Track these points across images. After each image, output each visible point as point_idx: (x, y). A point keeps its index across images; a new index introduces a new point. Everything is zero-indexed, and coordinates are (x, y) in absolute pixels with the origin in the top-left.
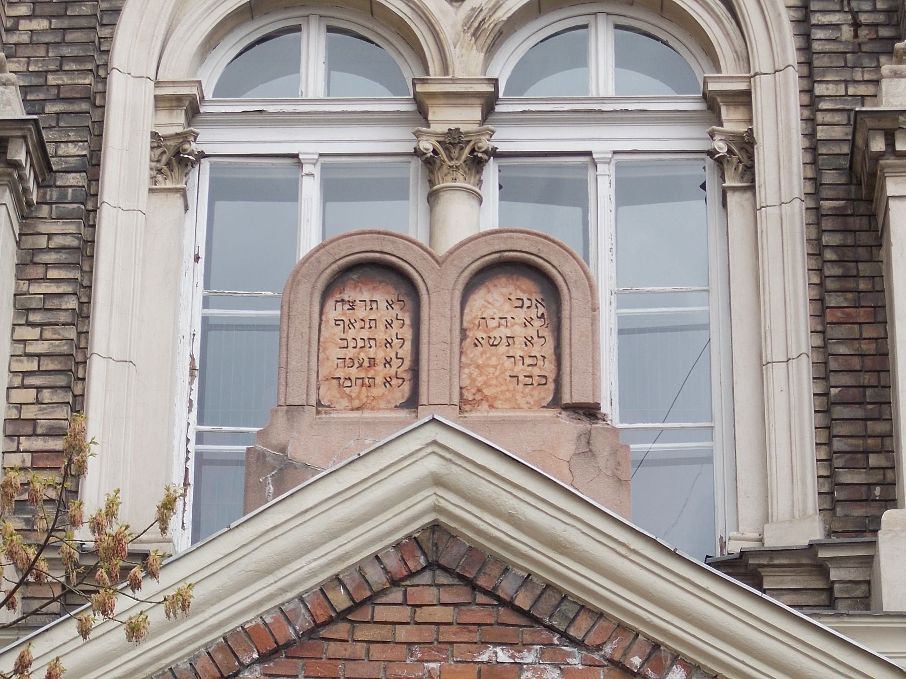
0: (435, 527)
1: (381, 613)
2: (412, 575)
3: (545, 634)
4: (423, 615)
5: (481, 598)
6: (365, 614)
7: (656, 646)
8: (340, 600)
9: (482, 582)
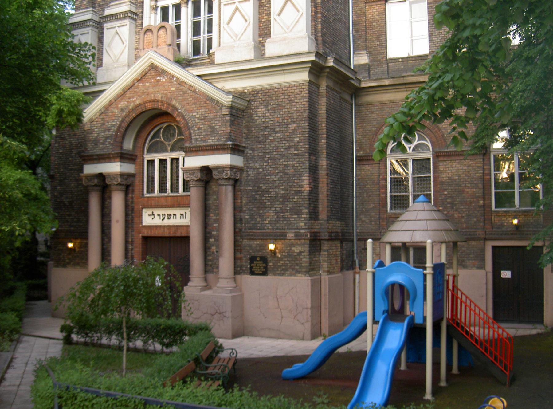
8: (144, 74)
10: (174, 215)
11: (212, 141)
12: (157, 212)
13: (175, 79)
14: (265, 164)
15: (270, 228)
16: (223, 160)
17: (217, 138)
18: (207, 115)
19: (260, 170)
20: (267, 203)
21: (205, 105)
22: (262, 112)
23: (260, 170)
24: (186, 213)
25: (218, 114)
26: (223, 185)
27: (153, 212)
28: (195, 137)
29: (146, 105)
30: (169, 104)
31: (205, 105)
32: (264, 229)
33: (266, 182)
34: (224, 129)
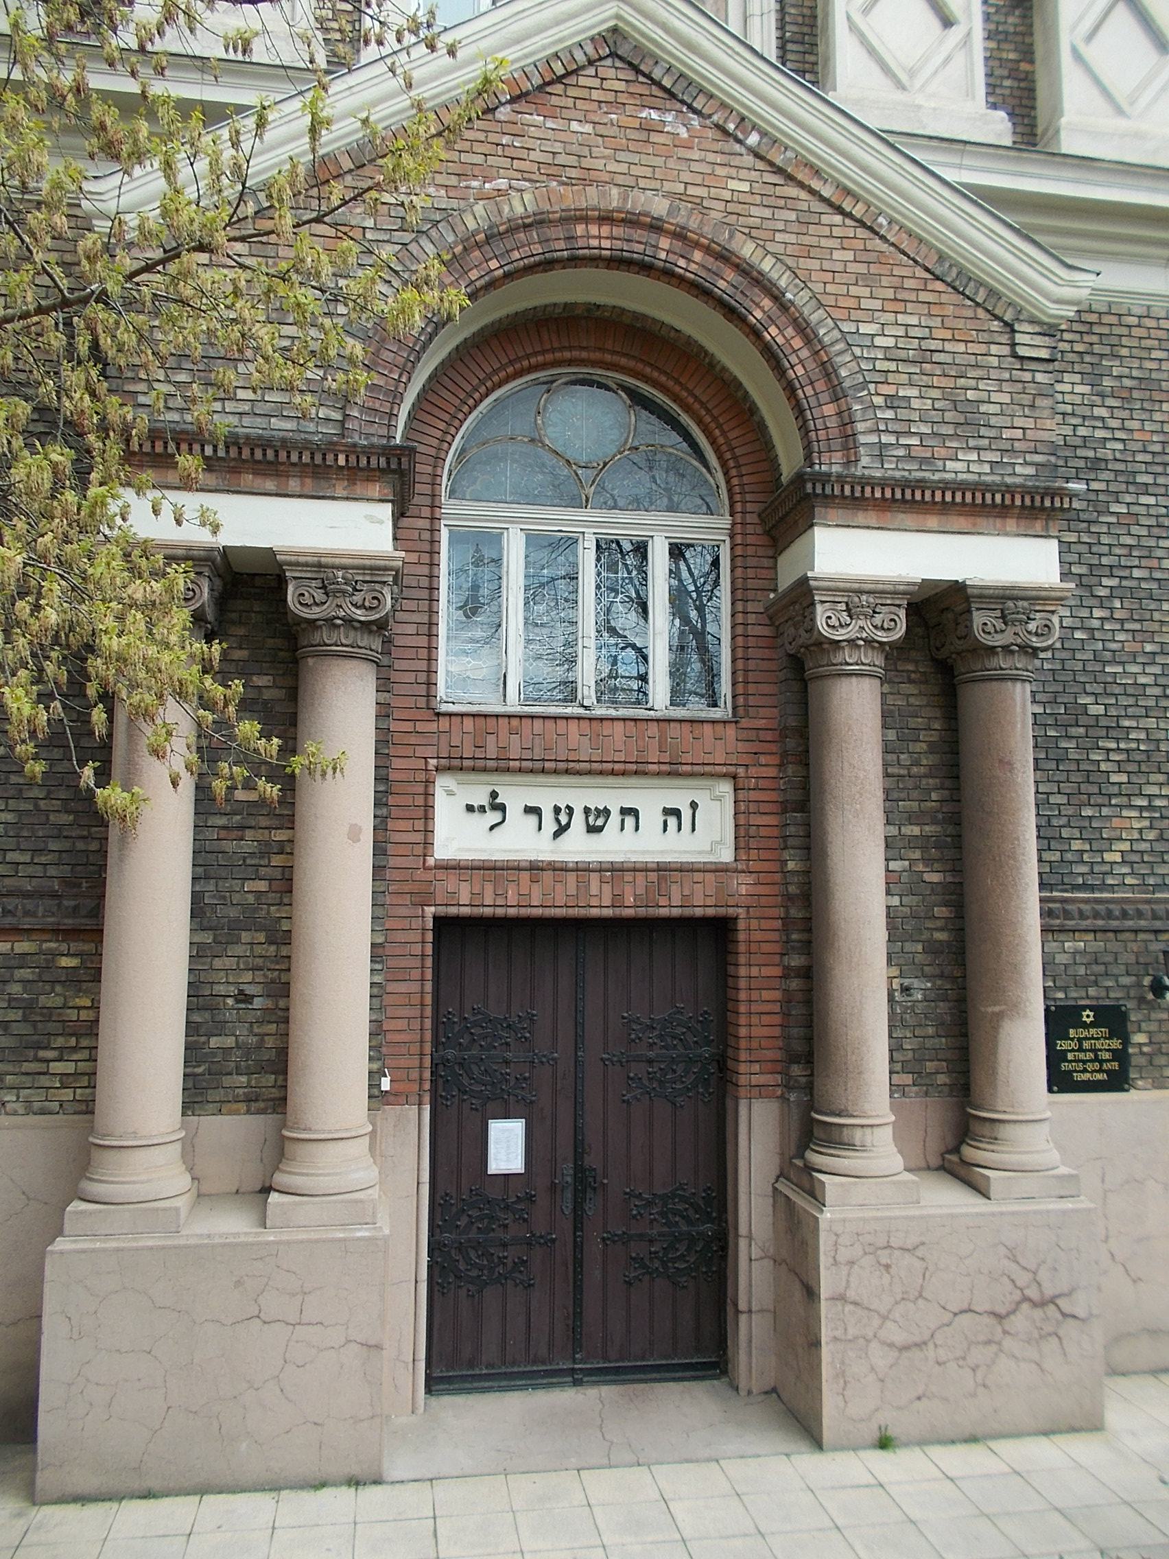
0: (615, 30)
1: (582, 81)
2: (601, 59)
3: (678, 106)
4: (606, 85)
5: (641, 79)
6: (572, 80)
7: (743, 119)
8: (560, 70)
9: (642, 67)
10: (625, 811)
11: (965, 465)
12: (515, 795)
13: (753, 139)
14: (1097, 613)
15: (1128, 880)
16: (1019, 560)
17: (995, 457)
18: (934, 345)
19: (1078, 635)
20: (1114, 778)
21: (924, 296)
22: (1078, 400)
23: (1078, 635)
24: (694, 806)
25: (994, 349)
26: (1015, 679)
27: (494, 795)
28: (873, 439)
29: (580, 229)
30: (725, 256)
31: (924, 296)
32: (1104, 887)
33: (1107, 688)
34: (1029, 423)
